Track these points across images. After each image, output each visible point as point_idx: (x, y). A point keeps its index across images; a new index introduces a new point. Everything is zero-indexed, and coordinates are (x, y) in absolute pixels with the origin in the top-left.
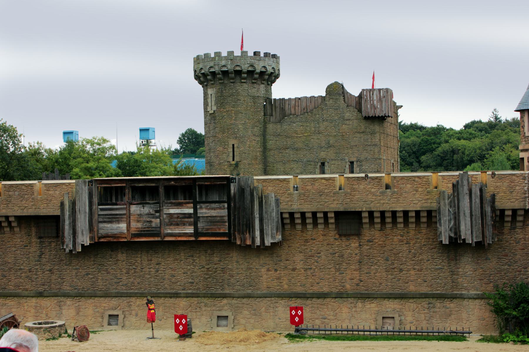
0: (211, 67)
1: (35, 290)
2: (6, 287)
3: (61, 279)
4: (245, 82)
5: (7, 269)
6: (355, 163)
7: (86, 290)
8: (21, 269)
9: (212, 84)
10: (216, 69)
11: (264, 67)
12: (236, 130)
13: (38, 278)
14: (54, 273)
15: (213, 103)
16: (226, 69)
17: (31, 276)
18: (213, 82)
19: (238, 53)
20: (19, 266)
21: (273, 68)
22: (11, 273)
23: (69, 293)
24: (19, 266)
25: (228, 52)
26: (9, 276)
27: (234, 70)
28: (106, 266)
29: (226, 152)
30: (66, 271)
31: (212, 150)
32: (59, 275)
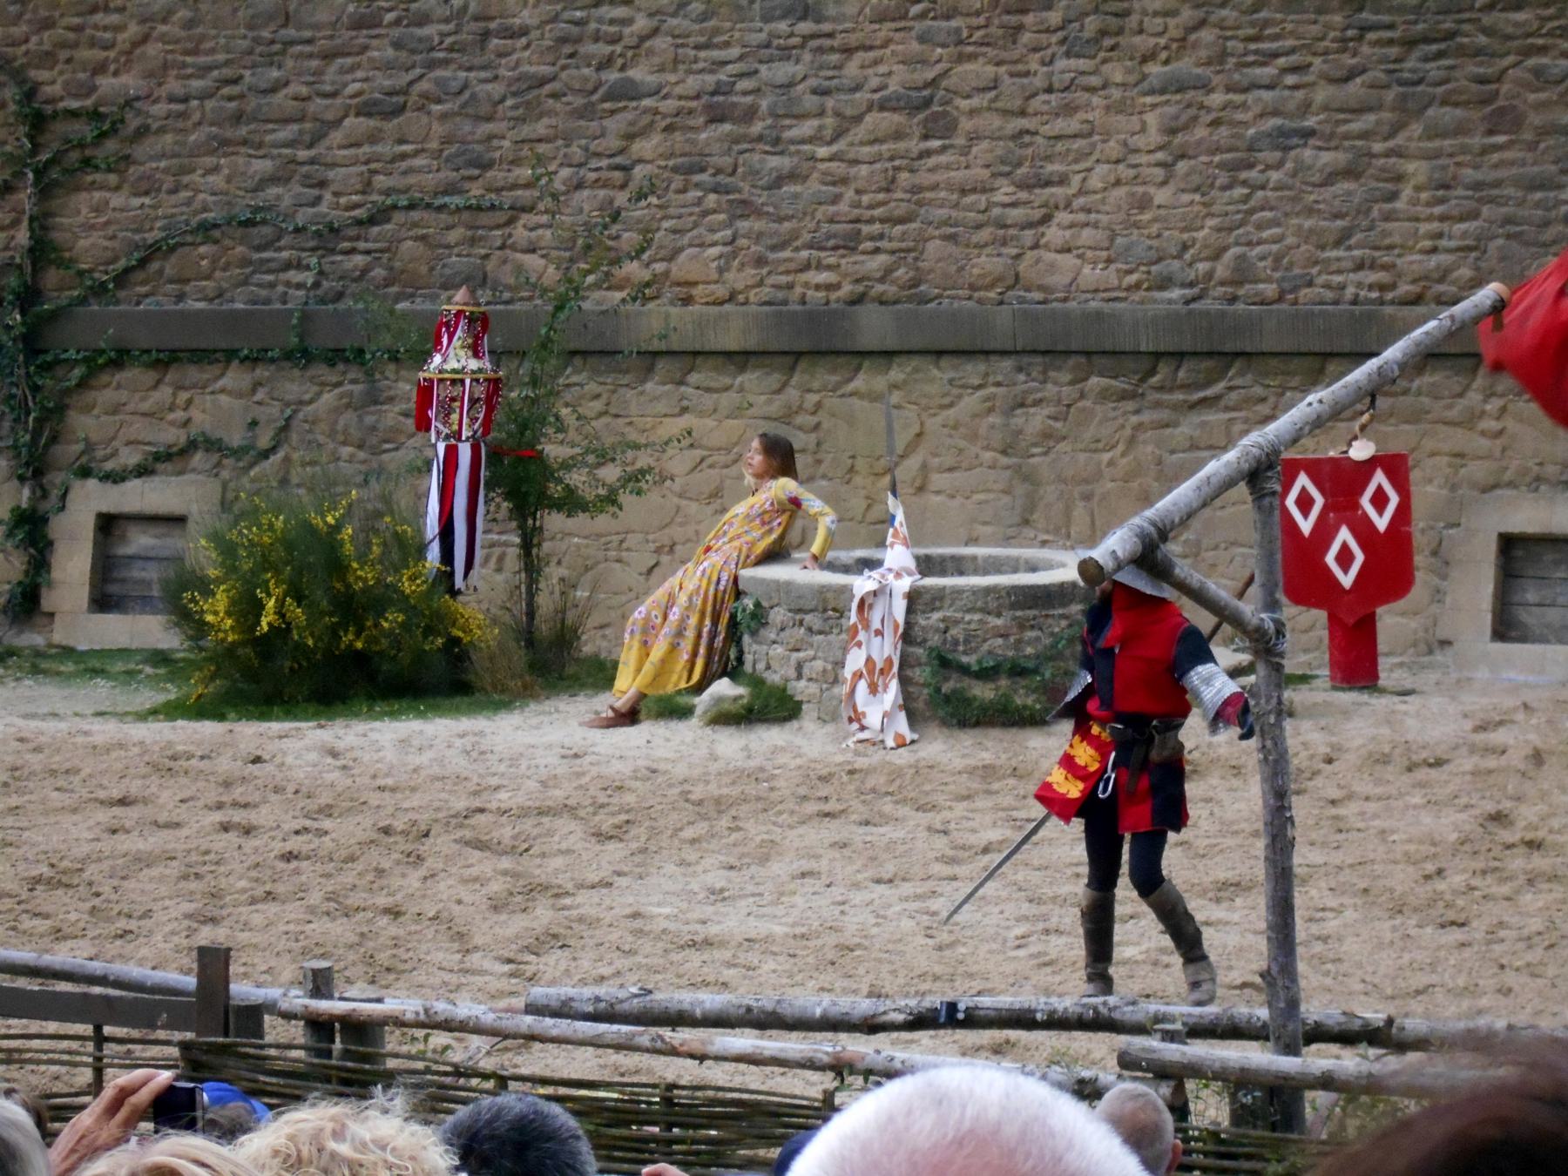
1: (766, 292)
2: (490, 266)
3: (1023, 185)
5: (496, 89)
7: (1270, 290)
8: (627, 92)
13: (793, 176)
14: (950, 129)
17: (727, 161)
20: (606, 63)
22: (541, 128)
23: (1098, 315)
24: (606, 63)
26: (516, 162)
28: (1478, 52)
30: (1069, 110)
32: (1000, 148)
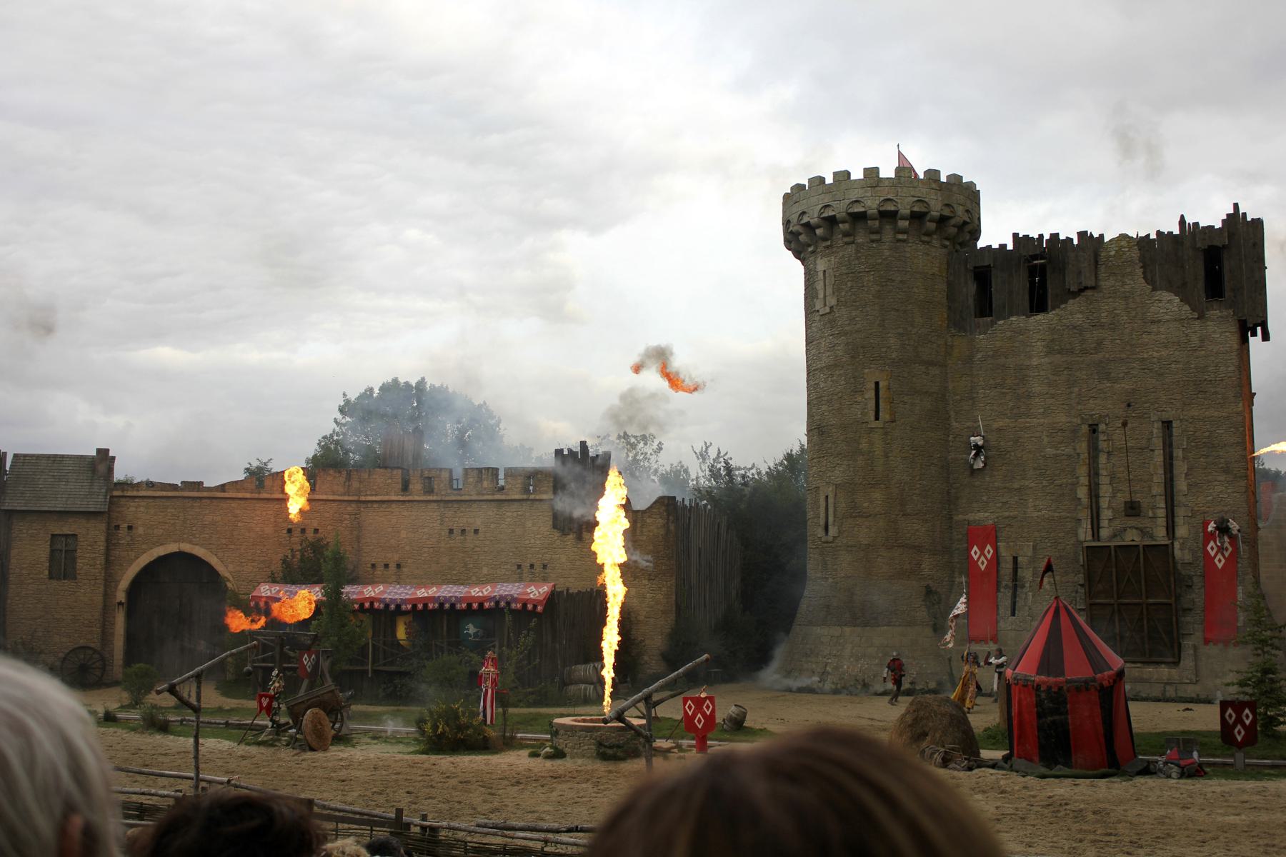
0: (826, 207)
4: (904, 241)
6: (1174, 425)
9: (827, 247)
10: (839, 210)
11: (947, 205)
12: (884, 350)
15: (829, 291)
16: (862, 210)
18: (829, 243)
19: (888, 172)
21: (967, 211)
25: (866, 170)
27: (880, 212)
29: (859, 399)
31: (826, 398)
